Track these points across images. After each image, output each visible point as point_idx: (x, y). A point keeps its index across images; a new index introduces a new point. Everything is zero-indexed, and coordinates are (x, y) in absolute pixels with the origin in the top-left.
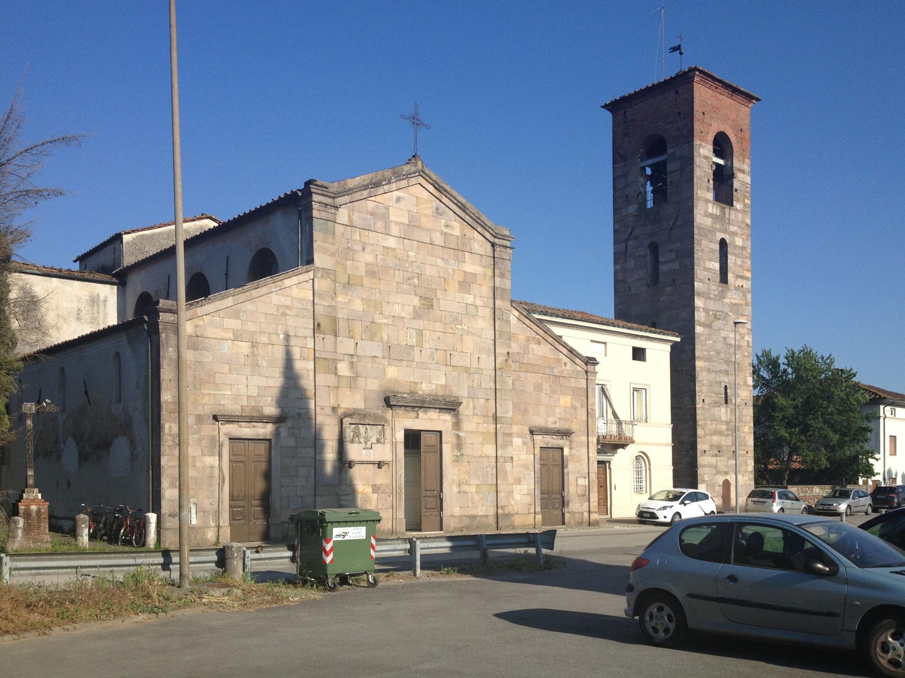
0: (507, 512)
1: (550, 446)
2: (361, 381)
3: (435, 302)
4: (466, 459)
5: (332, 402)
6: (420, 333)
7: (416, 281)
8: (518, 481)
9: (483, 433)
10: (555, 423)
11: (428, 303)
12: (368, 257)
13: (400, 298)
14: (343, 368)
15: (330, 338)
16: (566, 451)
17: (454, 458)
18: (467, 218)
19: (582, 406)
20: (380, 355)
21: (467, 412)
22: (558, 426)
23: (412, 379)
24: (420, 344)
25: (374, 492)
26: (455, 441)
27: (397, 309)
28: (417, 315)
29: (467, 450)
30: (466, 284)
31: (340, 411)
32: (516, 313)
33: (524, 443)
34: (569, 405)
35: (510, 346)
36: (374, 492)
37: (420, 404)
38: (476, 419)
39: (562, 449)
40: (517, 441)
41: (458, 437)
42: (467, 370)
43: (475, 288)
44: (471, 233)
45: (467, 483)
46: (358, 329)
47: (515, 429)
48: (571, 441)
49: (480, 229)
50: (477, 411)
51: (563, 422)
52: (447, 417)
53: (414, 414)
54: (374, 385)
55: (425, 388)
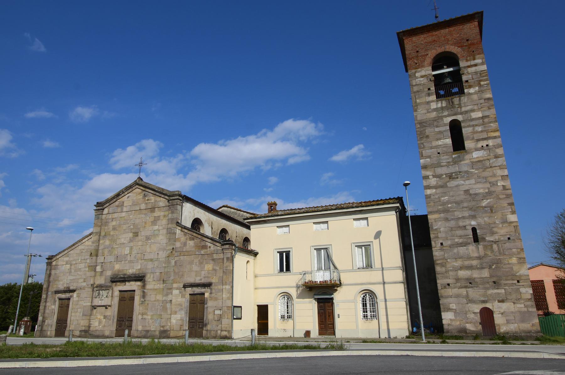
0: (165, 329)
1: (195, 293)
2: (104, 272)
3: (139, 234)
4: (146, 302)
5: (92, 282)
6: (131, 248)
7: (132, 227)
8: (176, 313)
9: (156, 289)
10: (201, 280)
11: (136, 234)
12: (114, 223)
13: (124, 236)
14: (99, 269)
15: (94, 258)
16: (207, 295)
17: (141, 302)
18: (157, 194)
19: (220, 268)
20: (113, 260)
21: (149, 280)
22: (204, 281)
23: (125, 268)
24: (130, 253)
25: (104, 318)
26: (142, 294)
27: (123, 241)
28: (131, 241)
29: (147, 298)
30: (155, 222)
31: (95, 285)
32: (180, 228)
33: (180, 292)
34: (211, 269)
35: (174, 245)
36: (104, 318)
37: (125, 279)
38: (154, 283)
39: (203, 294)
40: (176, 292)
41: (144, 292)
42: (151, 260)
43: (159, 222)
44: (158, 199)
45: (146, 314)
46: (106, 252)
47: (175, 285)
48: (211, 289)
49: (163, 196)
50: (155, 279)
51: (206, 279)
52: (139, 283)
53: (124, 284)
54: (109, 273)
55: (131, 272)
